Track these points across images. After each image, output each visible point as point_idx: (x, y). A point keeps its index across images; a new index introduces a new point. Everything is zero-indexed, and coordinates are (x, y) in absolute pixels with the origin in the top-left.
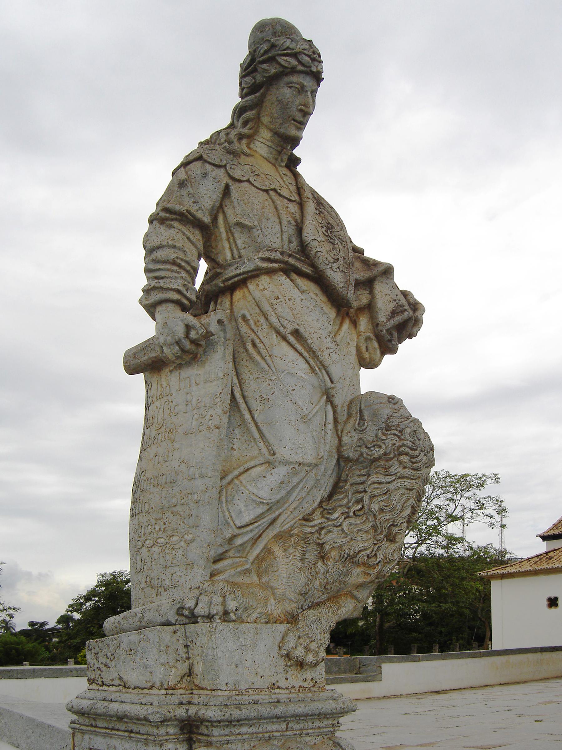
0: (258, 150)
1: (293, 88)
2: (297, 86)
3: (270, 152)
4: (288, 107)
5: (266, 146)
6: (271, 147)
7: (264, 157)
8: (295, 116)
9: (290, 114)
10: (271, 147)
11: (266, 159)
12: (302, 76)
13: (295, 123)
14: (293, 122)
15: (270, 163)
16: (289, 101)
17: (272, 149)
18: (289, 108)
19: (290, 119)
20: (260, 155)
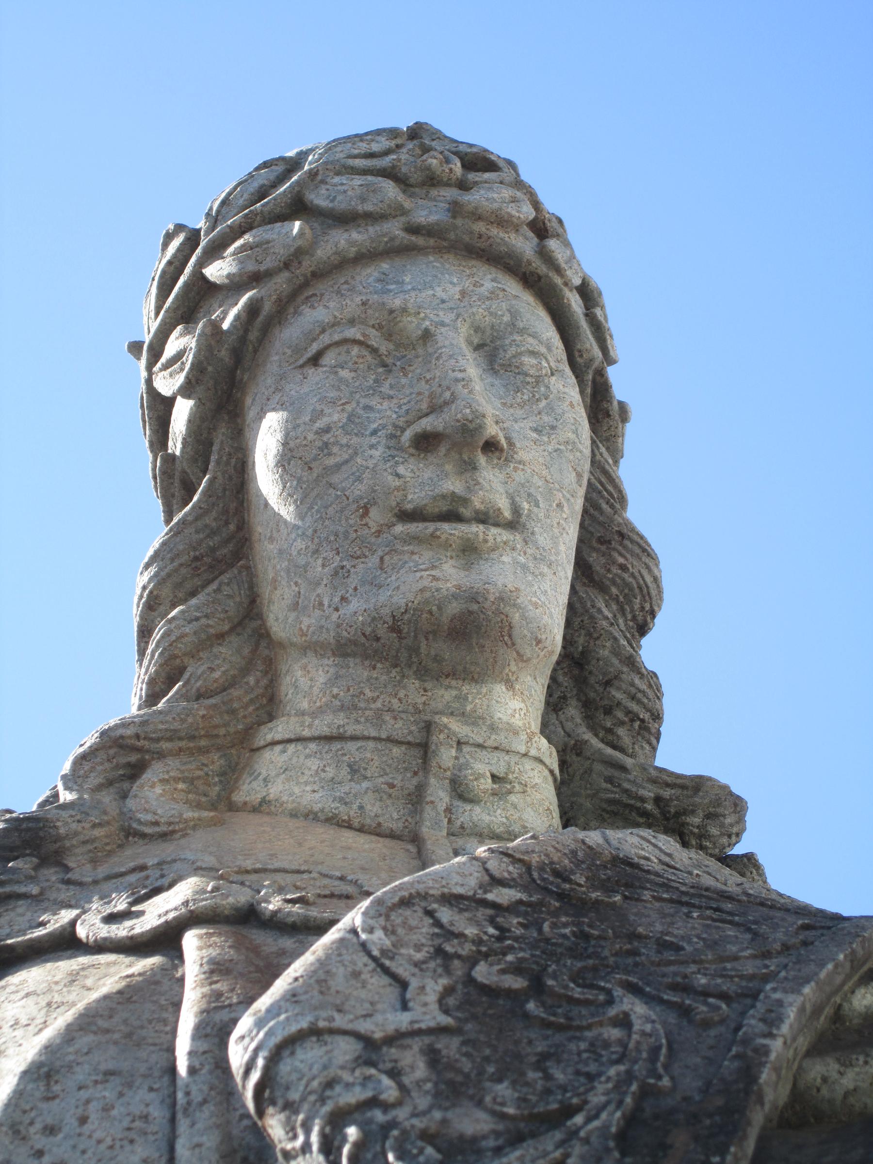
0: (275, 790)
1: (329, 359)
2: (352, 333)
3: (345, 771)
4: (331, 461)
5: (313, 746)
6: (340, 738)
7: (311, 816)
8: (403, 489)
9: (359, 490)
10: (340, 738)
11: (335, 821)
12: (369, 275)
13: (414, 528)
14: (399, 528)
15: (377, 832)
16: (327, 430)
17: (352, 746)
18: (338, 467)
19: (375, 515)
20: (294, 815)
